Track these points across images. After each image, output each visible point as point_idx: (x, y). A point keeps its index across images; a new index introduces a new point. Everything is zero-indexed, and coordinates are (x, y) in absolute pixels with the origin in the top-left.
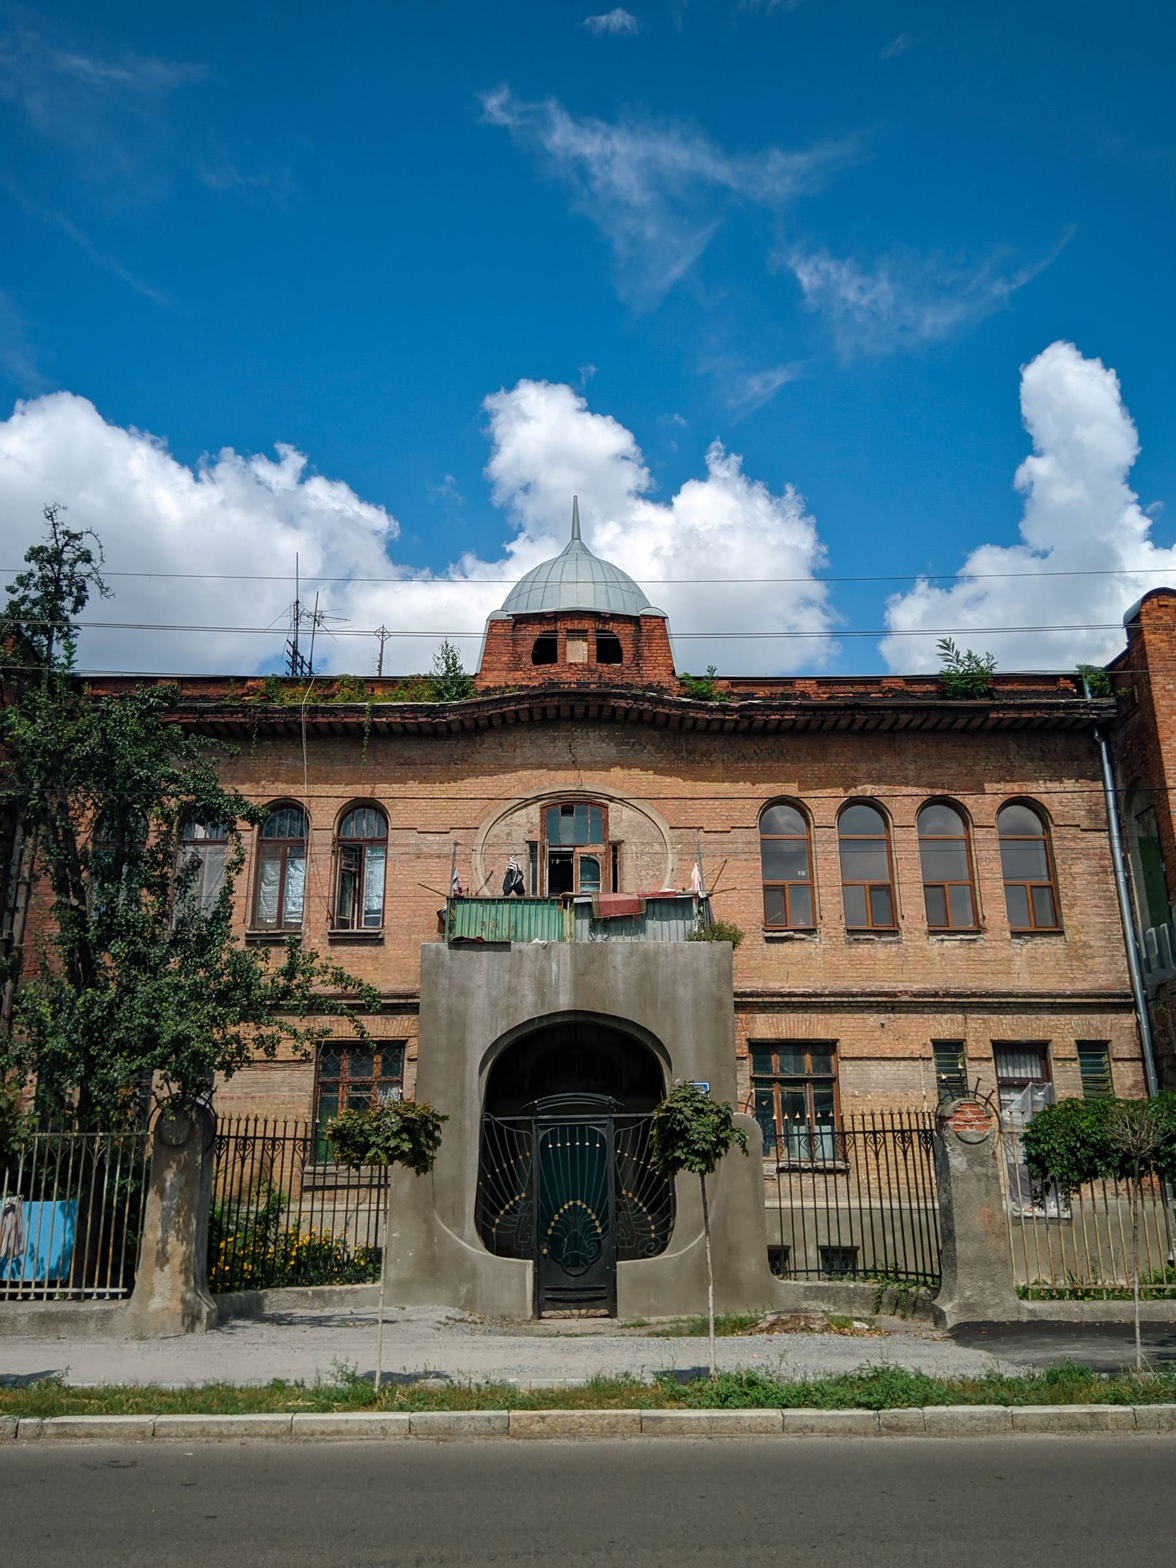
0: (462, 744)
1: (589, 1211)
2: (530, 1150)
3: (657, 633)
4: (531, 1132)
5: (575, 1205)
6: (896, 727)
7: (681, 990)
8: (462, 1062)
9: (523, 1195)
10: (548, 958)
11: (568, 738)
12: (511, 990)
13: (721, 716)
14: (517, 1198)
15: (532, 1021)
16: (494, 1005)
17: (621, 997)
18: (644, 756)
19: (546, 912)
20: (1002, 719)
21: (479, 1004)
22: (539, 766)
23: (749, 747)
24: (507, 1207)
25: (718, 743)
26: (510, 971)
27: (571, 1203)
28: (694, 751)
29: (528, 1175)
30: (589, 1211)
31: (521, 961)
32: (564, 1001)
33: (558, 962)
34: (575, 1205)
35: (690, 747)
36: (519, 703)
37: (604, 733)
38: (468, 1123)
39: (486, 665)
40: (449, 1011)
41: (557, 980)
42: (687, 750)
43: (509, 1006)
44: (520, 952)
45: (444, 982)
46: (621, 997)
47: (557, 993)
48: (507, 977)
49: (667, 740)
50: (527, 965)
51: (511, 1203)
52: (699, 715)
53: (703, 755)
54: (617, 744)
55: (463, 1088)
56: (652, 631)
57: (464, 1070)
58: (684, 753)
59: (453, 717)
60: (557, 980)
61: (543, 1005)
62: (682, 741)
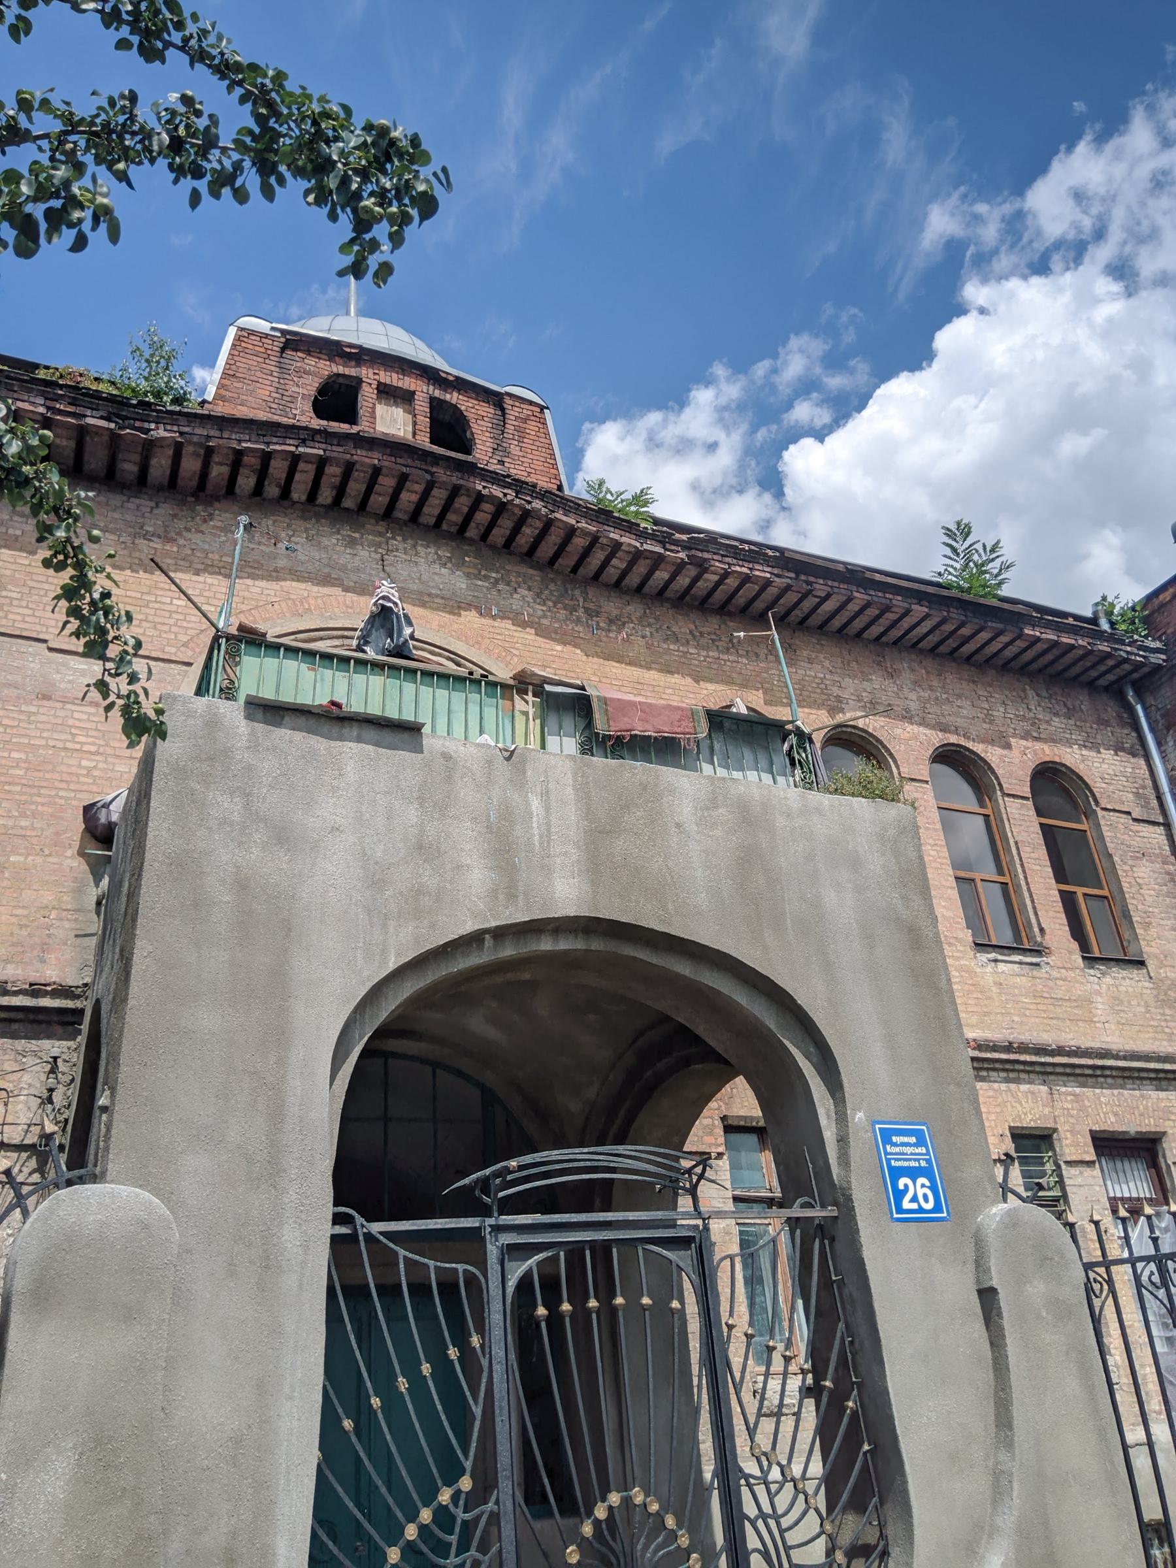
0: (165, 509)
1: (670, 1521)
2: (481, 1330)
3: (532, 427)
4: (482, 1265)
5: (627, 1501)
6: (884, 639)
7: (830, 898)
8: (278, 1036)
9: (466, 1484)
10: (519, 780)
11: (379, 545)
12: (424, 850)
13: (658, 549)
14: (445, 1496)
15: (475, 939)
16: (376, 881)
17: (702, 899)
18: (515, 602)
19: (474, 709)
20: (1038, 639)
21: (331, 875)
22: (325, 580)
23: (683, 625)
24: (411, 1532)
25: (635, 609)
26: (421, 800)
27: (614, 1498)
28: (598, 614)
29: (478, 1411)
30: (670, 1521)
31: (449, 779)
32: (566, 894)
33: (546, 795)
34: (627, 1501)
35: (592, 606)
36: (304, 442)
37: (445, 553)
38: (290, 1237)
39: (223, 392)
40: (242, 885)
41: (546, 836)
42: (586, 610)
43: (420, 891)
44: (447, 757)
45: (225, 804)
46: (702, 899)
47: (547, 870)
48: (412, 815)
49: (552, 587)
50: (466, 793)
51: (426, 1515)
52: (623, 540)
53: (611, 622)
54: (468, 575)
55: (277, 1116)
56: (525, 421)
57: (282, 1062)
58: (580, 612)
59: (162, 433)
60: (546, 836)
61: (512, 896)
62: (577, 593)
